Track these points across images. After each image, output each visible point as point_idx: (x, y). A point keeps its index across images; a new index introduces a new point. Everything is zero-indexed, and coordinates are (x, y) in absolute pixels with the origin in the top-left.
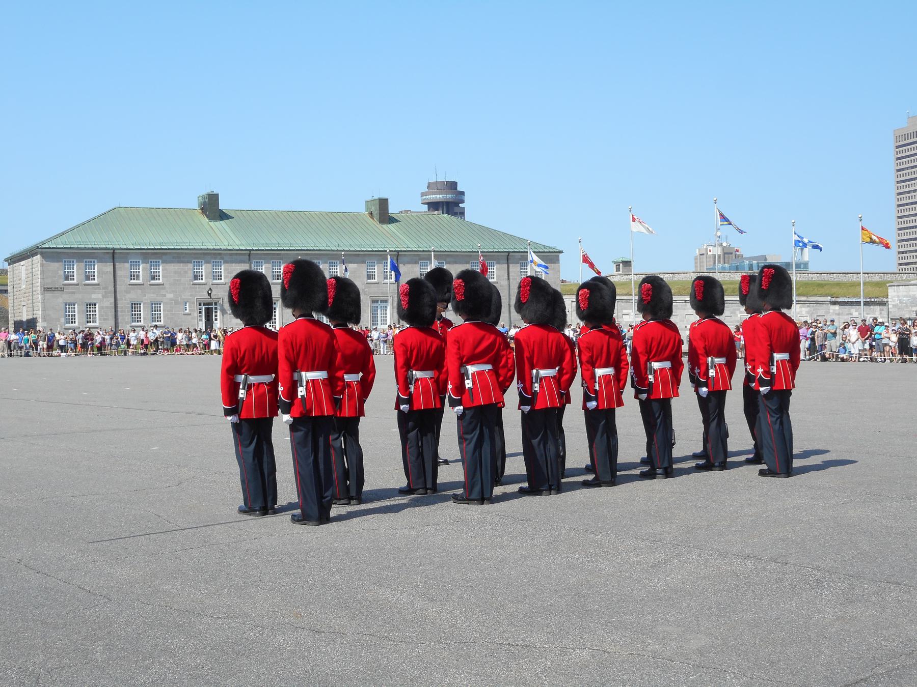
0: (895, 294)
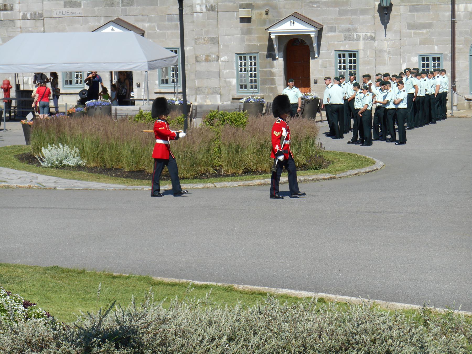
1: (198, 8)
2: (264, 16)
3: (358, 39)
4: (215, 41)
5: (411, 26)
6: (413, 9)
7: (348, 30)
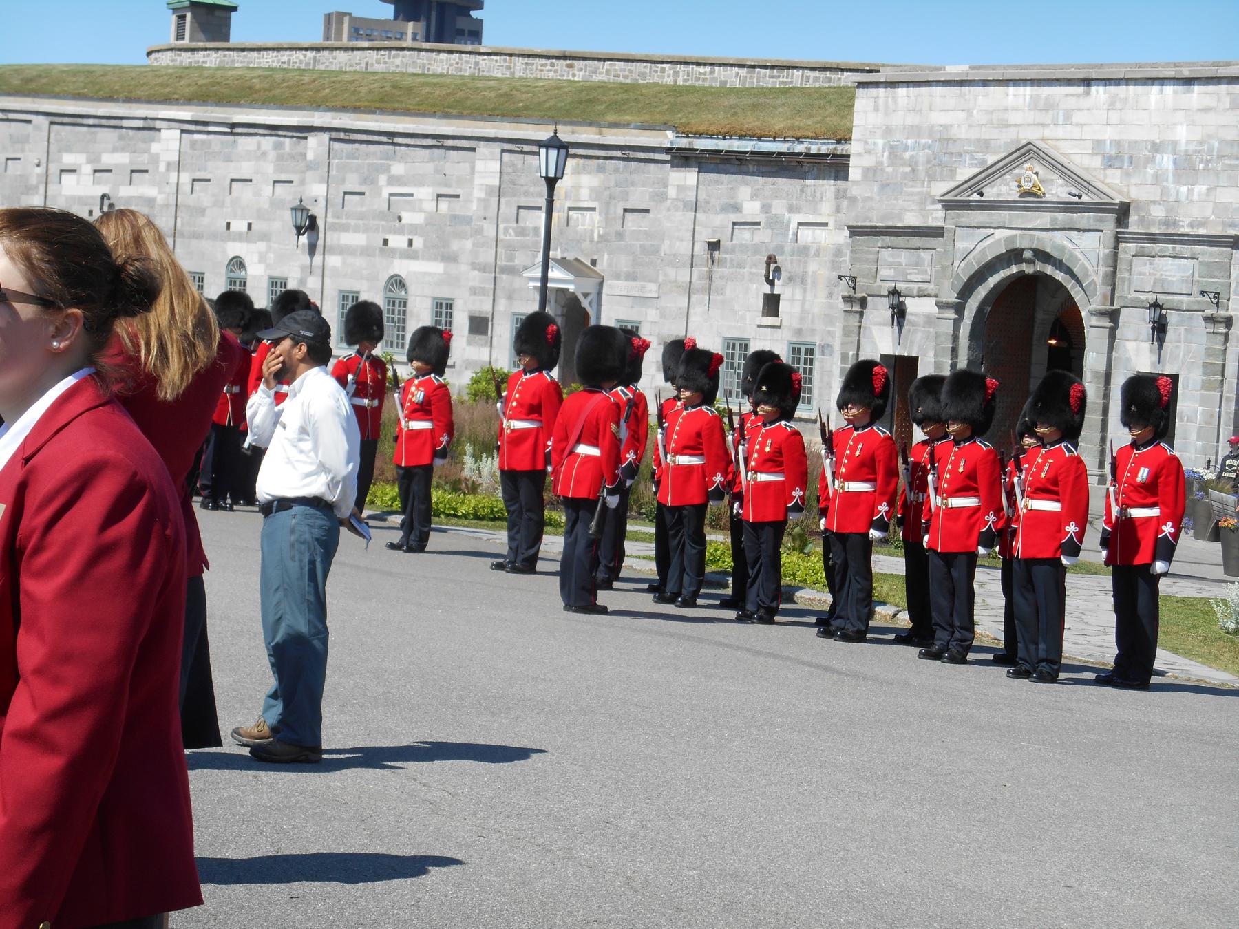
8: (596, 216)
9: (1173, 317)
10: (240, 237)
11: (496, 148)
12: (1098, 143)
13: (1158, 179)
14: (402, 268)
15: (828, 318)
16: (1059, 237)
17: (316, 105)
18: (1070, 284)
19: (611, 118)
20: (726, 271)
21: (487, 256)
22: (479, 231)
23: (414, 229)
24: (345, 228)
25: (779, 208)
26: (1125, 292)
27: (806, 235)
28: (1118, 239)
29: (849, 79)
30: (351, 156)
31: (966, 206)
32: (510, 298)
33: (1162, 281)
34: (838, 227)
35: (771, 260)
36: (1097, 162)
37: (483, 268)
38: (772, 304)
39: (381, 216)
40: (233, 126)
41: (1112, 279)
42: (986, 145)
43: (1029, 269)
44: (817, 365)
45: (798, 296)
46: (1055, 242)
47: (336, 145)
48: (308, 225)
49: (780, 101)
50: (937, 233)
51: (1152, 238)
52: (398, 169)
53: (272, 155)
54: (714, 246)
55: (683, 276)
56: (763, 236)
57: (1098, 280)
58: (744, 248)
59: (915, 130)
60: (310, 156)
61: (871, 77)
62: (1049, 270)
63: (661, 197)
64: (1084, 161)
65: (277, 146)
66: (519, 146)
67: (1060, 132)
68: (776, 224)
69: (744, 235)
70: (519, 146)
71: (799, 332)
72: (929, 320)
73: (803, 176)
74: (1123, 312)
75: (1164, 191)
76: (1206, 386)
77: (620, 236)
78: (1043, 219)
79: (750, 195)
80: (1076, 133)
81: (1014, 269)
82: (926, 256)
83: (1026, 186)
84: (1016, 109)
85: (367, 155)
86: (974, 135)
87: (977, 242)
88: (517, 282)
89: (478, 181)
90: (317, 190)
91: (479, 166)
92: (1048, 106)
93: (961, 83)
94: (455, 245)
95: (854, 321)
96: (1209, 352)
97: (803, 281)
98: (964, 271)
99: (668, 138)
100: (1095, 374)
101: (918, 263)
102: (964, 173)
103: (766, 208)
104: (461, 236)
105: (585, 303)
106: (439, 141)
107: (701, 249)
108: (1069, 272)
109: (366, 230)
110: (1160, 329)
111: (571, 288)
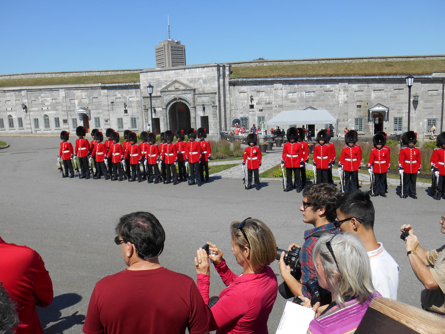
0: (144, 78)
1: (341, 102)
2: (366, 104)
3: (403, 113)
4: (347, 114)
5: (424, 108)
6: (426, 102)
7: (399, 110)
8: (87, 100)
9: (206, 107)
10: (10, 111)
11: (64, 90)
12: (188, 79)
13: (200, 84)
14: (47, 113)
15: (138, 113)
16: (183, 95)
17: (22, 85)
18: (186, 103)
19: (86, 82)
20: (116, 106)
21: (65, 109)
22: (63, 105)
23: (48, 106)
24: (33, 107)
25: (124, 95)
26: (197, 103)
27: (131, 99)
28: (194, 95)
29: (138, 72)
30: (31, 94)
31: (165, 91)
32: (71, 115)
33: (203, 101)
34: (137, 97)
35: (125, 104)
36: (188, 82)
37: (64, 111)
38: (126, 111)
39: (40, 104)
40: (4, 91)
41: (194, 101)
42: (167, 81)
43: (178, 101)
44: (137, 121)
45: (131, 109)
46: (183, 96)
47: (28, 92)
48: (25, 108)
49: (118, 77)
50: (160, 97)
51: (200, 94)
52: (43, 95)
53: (14, 95)
54: (112, 103)
55: (107, 108)
56: (122, 100)
57: (192, 102)
58: (119, 102)
59: (153, 80)
60: (23, 95)
61: (142, 71)
62: (182, 101)
63: (100, 95)
64: (187, 83)
65: (15, 94)
66: (69, 89)
67: (180, 78)
68: (124, 98)
69: (118, 100)
70: (69, 89)
71: (132, 116)
72: (161, 111)
73: (128, 89)
74: (197, 107)
75: (202, 86)
76: (214, 117)
77: (92, 102)
78: (180, 92)
79: (118, 93)
80: (184, 78)
81: (175, 101)
82: (158, 101)
83: (176, 87)
84: (172, 74)
85: (35, 93)
86: (164, 79)
87: (168, 98)
88: (72, 113)
89: (60, 96)
90: (25, 101)
91: (60, 93)
92: (178, 74)
93: (160, 71)
94: (57, 108)
95: (146, 113)
96: (214, 112)
97: (131, 107)
98: (166, 102)
99: (100, 85)
100: (193, 117)
101: (157, 102)
102: (164, 86)
103: (122, 95)
104: (58, 106)
105: (88, 115)
106: (51, 90)
107: (110, 103)
108: (186, 101)
109: (37, 107)
110: (204, 109)
111: (85, 113)
